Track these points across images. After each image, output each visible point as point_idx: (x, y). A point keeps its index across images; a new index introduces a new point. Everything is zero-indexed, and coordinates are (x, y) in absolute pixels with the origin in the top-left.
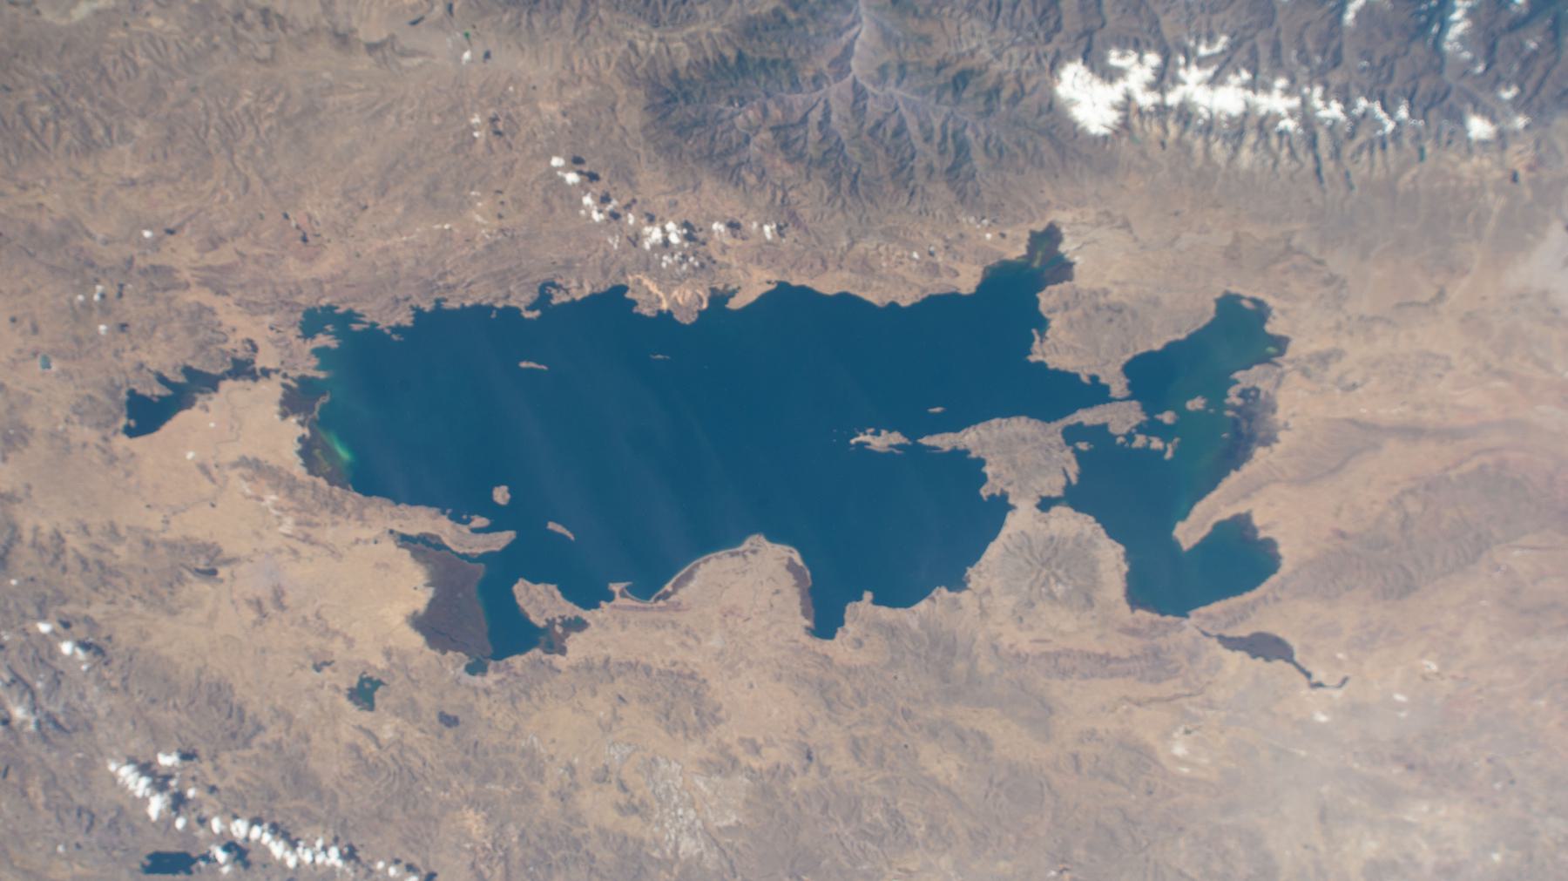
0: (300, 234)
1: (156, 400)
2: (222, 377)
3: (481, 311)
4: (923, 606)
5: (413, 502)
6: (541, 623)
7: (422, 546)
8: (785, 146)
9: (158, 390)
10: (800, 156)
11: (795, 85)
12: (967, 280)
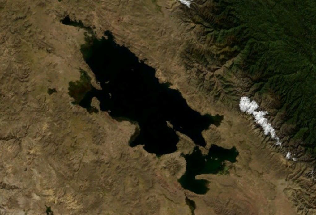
0: (119, 19)
1: (71, 21)
3: (133, 55)
4: (150, 154)
8: (197, 73)
9: (73, 20)
10: (198, 76)
11: (206, 67)
12: (203, 113)
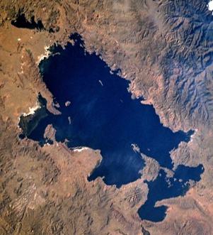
2: (45, 29)
5: (50, 90)
6: (45, 137)
7: (42, 100)
12: (175, 130)
